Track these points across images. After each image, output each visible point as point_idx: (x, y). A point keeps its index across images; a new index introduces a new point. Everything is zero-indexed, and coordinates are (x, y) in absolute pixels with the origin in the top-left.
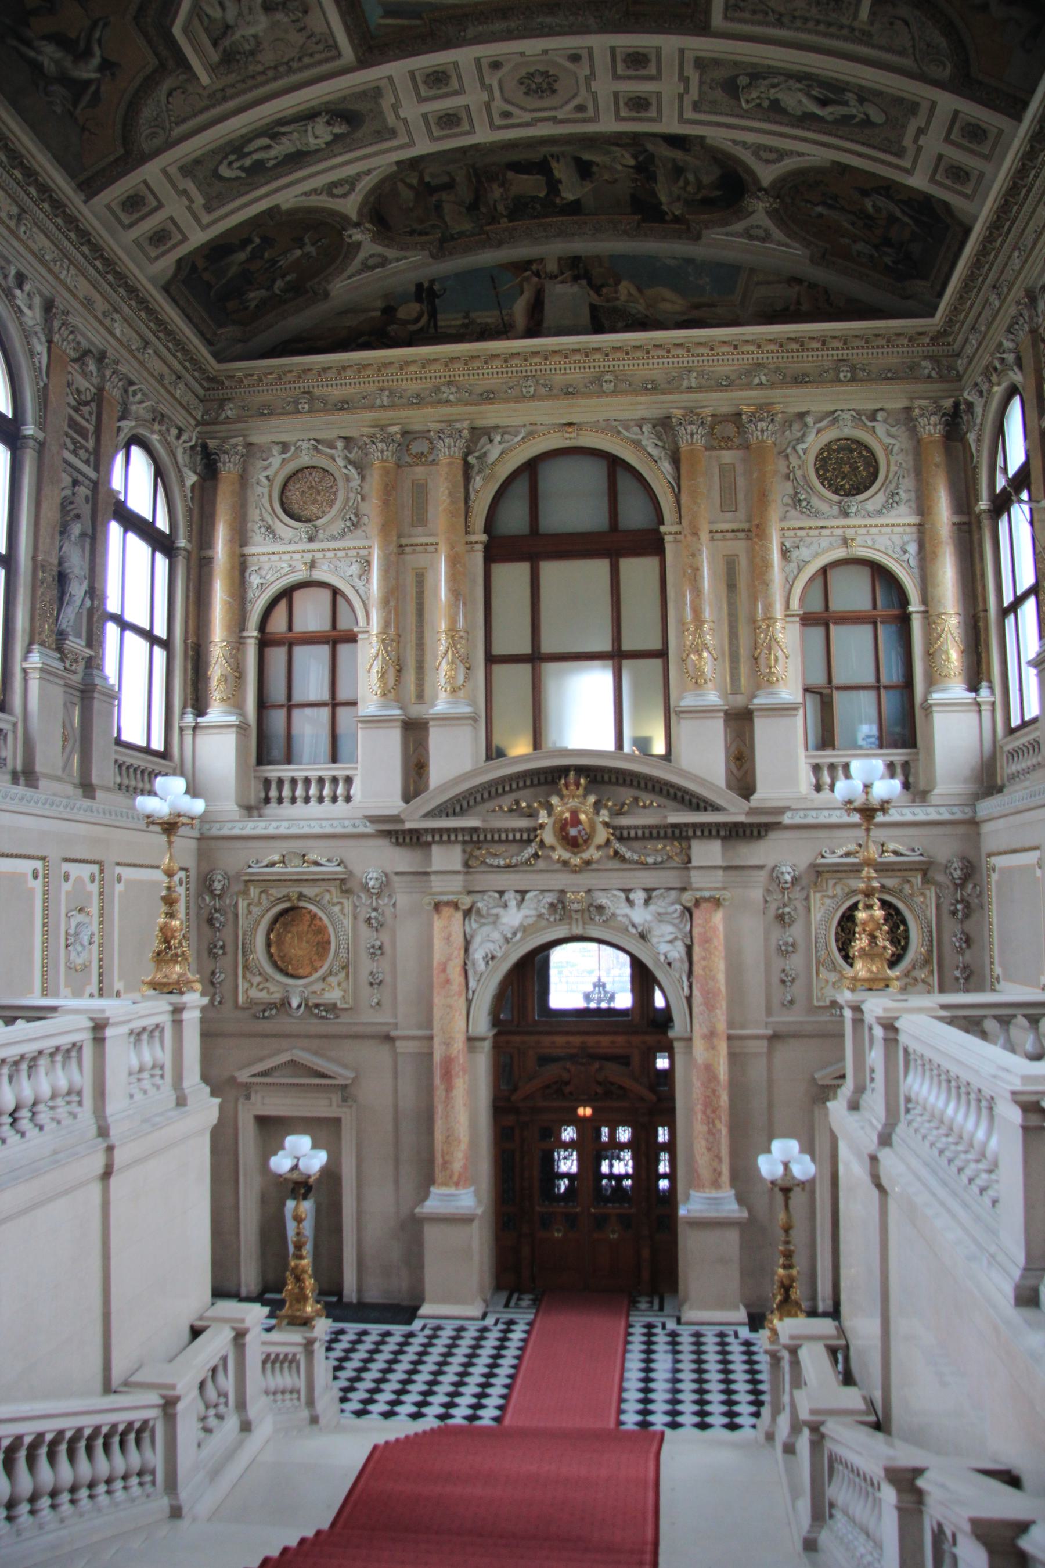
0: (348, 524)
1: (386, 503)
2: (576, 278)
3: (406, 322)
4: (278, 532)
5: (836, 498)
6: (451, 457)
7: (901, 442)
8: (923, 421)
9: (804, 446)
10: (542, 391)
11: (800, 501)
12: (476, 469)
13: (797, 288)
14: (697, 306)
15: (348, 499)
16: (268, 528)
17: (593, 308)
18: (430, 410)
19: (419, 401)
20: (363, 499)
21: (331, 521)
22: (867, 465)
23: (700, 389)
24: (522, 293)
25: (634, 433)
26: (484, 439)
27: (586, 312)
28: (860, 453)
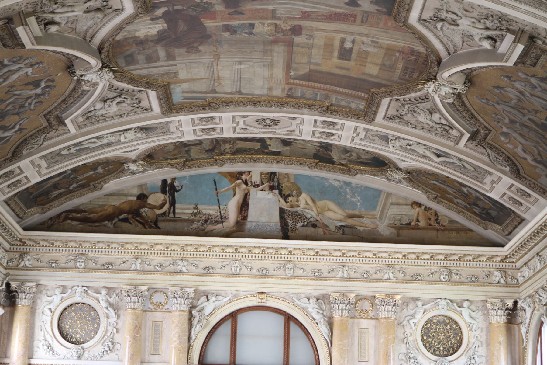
0: (107, 349)
1: (135, 338)
2: (272, 188)
3: (153, 207)
4: (55, 349)
5: (434, 357)
6: (181, 311)
7: (480, 321)
8: (493, 313)
9: (414, 321)
10: (245, 271)
11: (410, 358)
12: (197, 319)
13: (418, 209)
14: (351, 217)
15: (107, 331)
16: (49, 346)
17: (282, 211)
18: (168, 277)
19: (160, 269)
20: (117, 332)
21: (94, 346)
22: (456, 334)
23: (350, 279)
24: (234, 195)
25: (304, 303)
26: (204, 299)
27: (277, 213)
28: (451, 326)
